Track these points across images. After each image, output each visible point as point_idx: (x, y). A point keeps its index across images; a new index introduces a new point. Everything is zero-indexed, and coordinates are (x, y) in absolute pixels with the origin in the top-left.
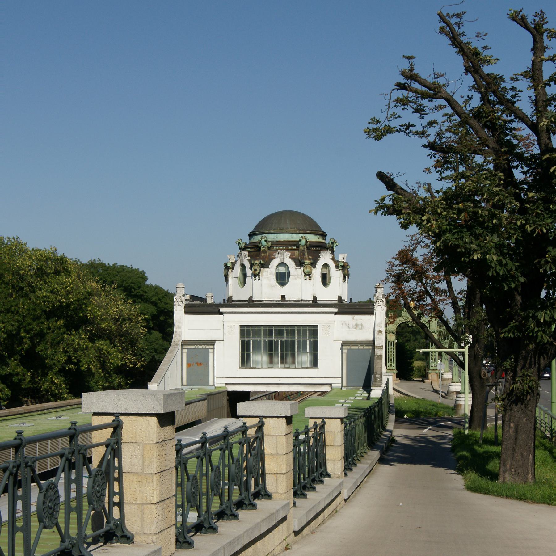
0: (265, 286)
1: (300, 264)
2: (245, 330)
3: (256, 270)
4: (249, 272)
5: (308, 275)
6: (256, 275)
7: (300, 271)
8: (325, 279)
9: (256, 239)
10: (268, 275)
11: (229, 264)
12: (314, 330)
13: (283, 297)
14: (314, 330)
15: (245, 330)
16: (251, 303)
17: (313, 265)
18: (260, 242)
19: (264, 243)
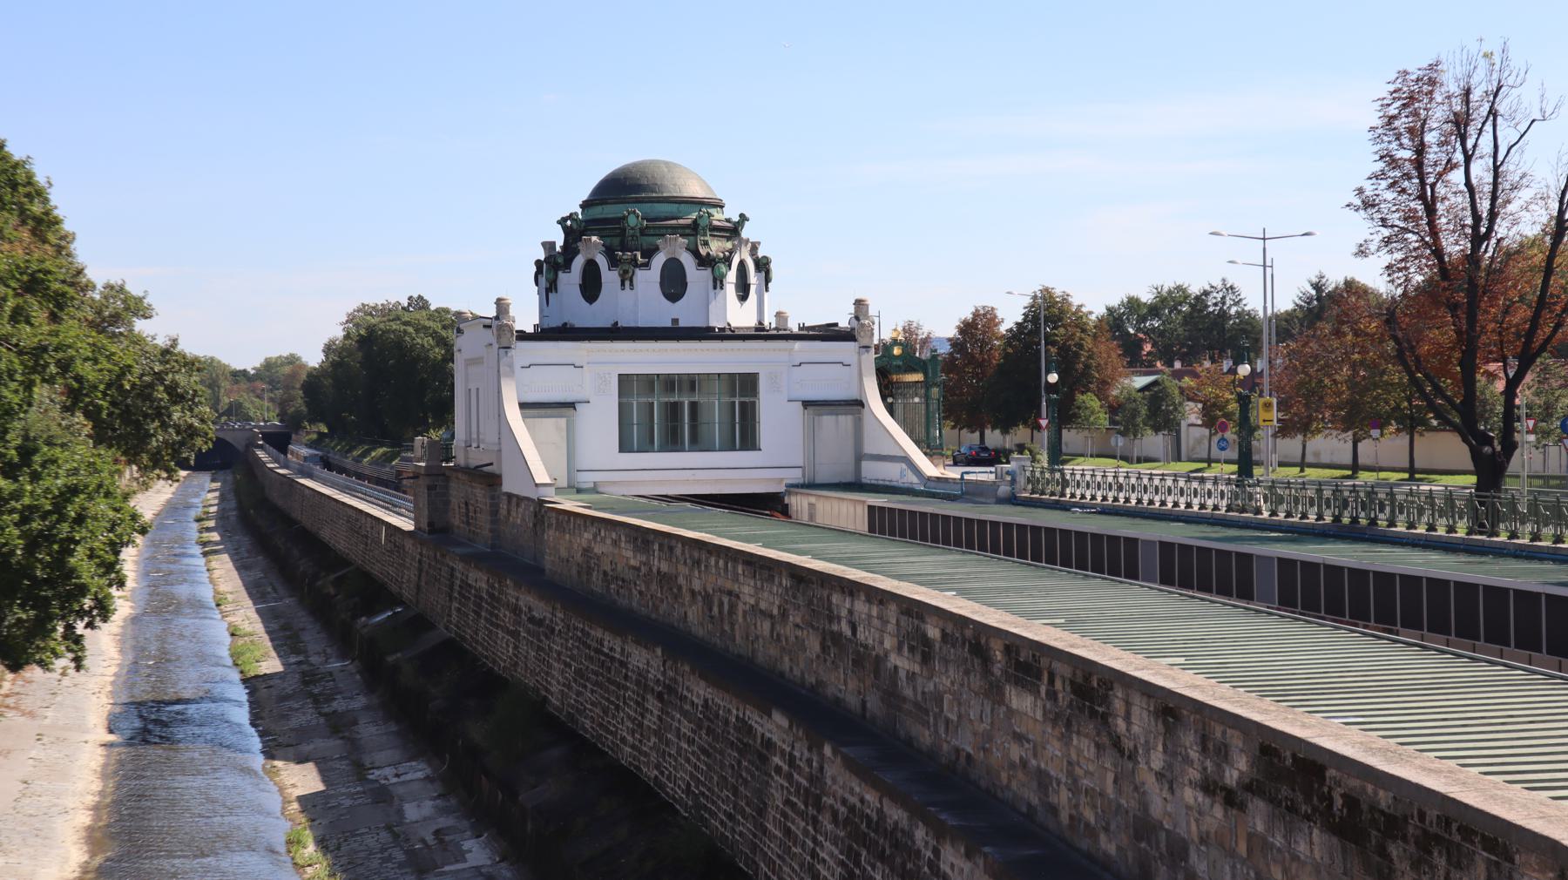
0: (641, 297)
1: (705, 262)
2: (625, 381)
3: (626, 272)
4: (610, 277)
5: (718, 282)
6: (626, 280)
7: (706, 274)
8: (743, 291)
9: (610, 211)
10: (649, 279)
11: (560, 260)
12: (746, 384)
13: (675, 321)
14: (746, 384)
15: (625, 381)
16: (615, 333)
17: (728, 261)
18: (624, 218)
19: (632, 221)
